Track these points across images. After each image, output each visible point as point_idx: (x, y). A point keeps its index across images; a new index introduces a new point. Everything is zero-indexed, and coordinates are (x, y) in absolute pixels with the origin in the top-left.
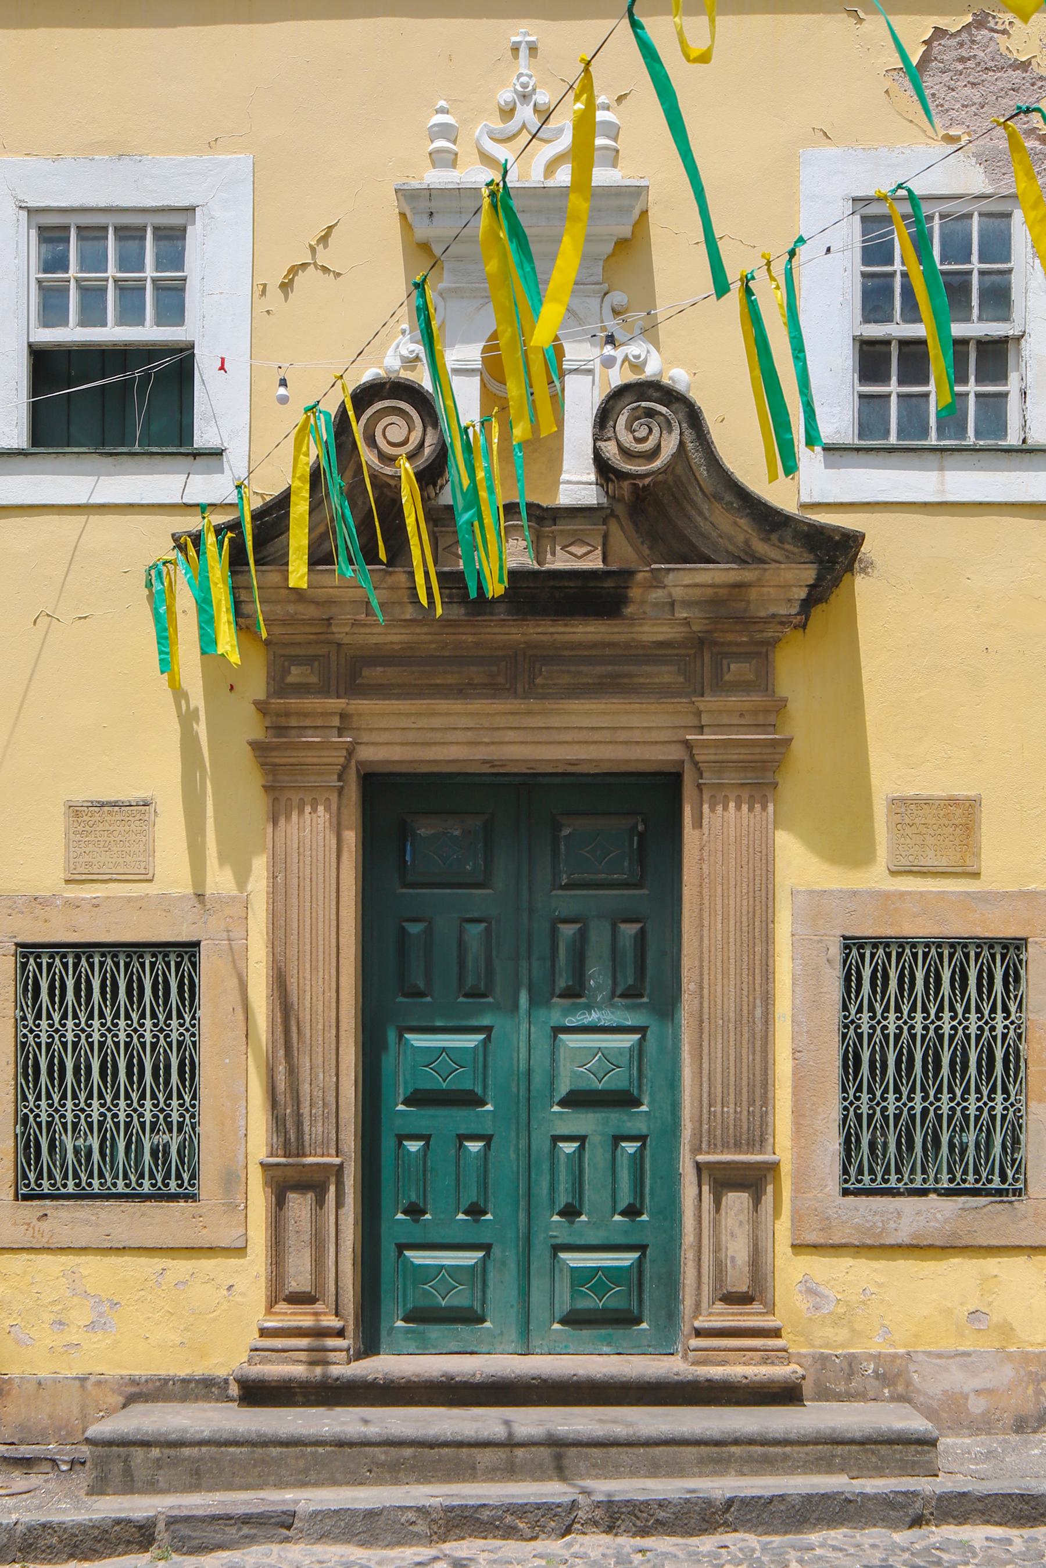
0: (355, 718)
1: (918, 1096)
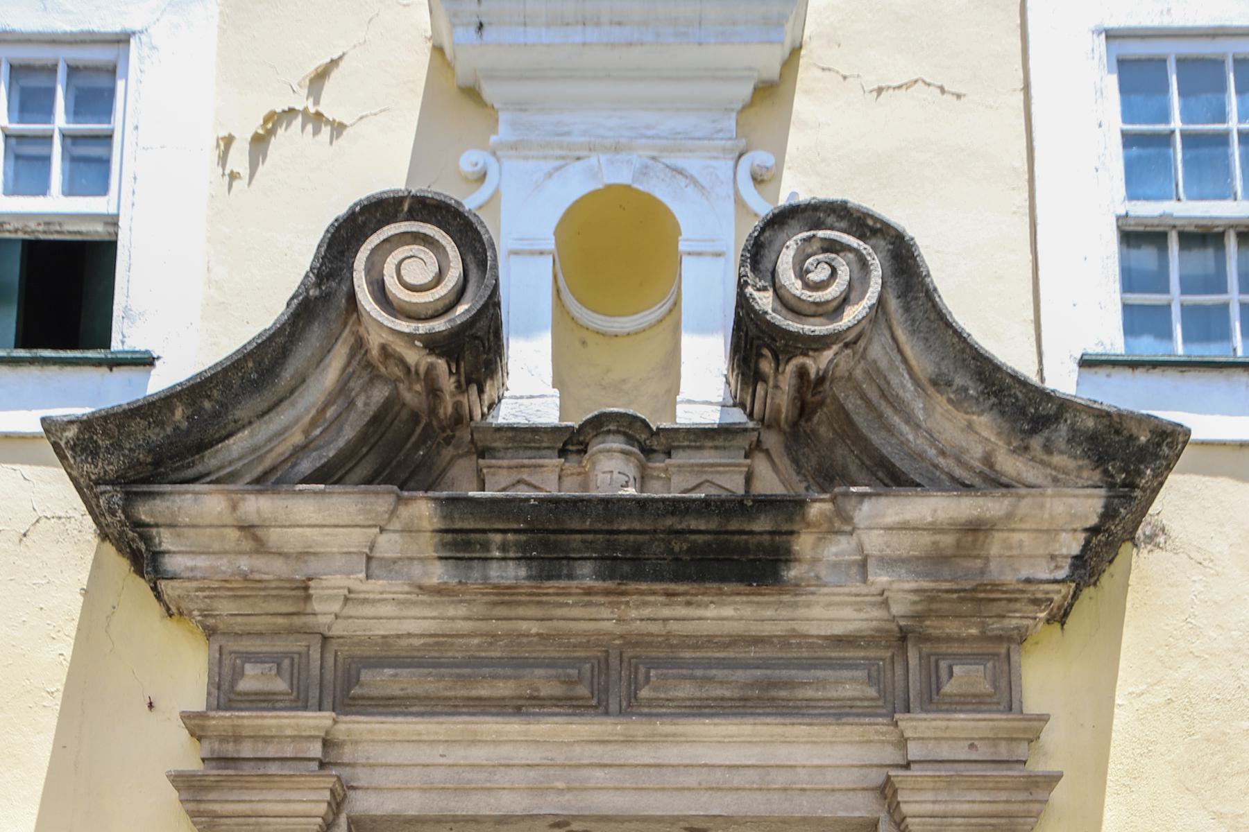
0: (347, 749)
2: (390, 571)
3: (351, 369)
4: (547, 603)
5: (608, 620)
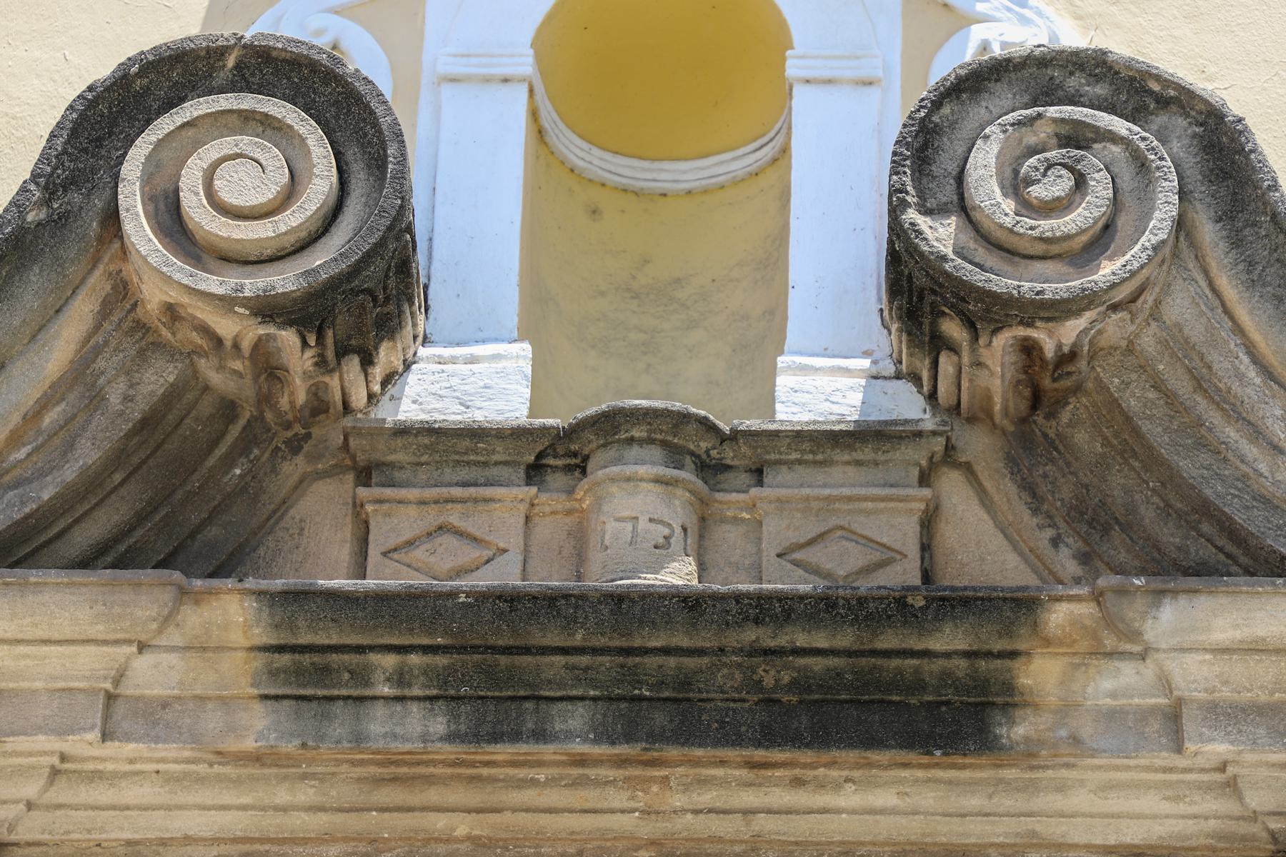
2: (155, 724)
3: (99, 338)
4: (492, 780)
5: (623, 811)
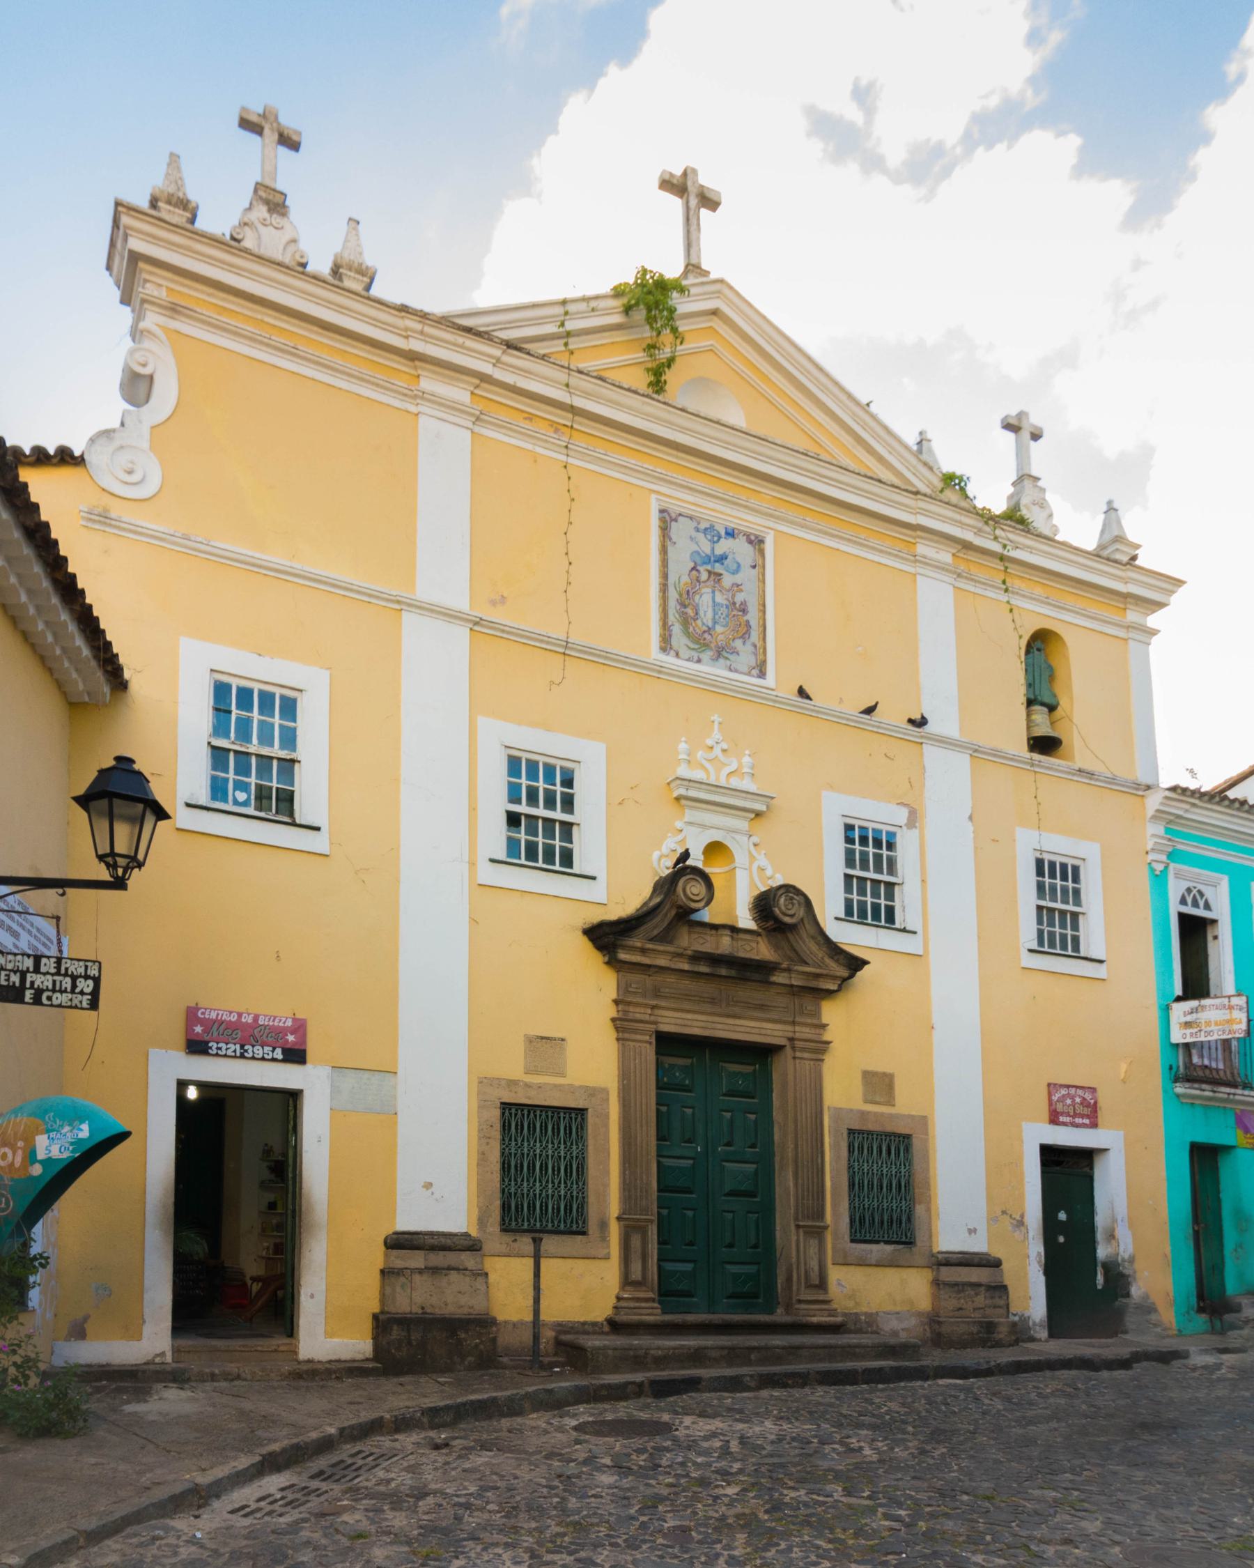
1: (876, 1200)
